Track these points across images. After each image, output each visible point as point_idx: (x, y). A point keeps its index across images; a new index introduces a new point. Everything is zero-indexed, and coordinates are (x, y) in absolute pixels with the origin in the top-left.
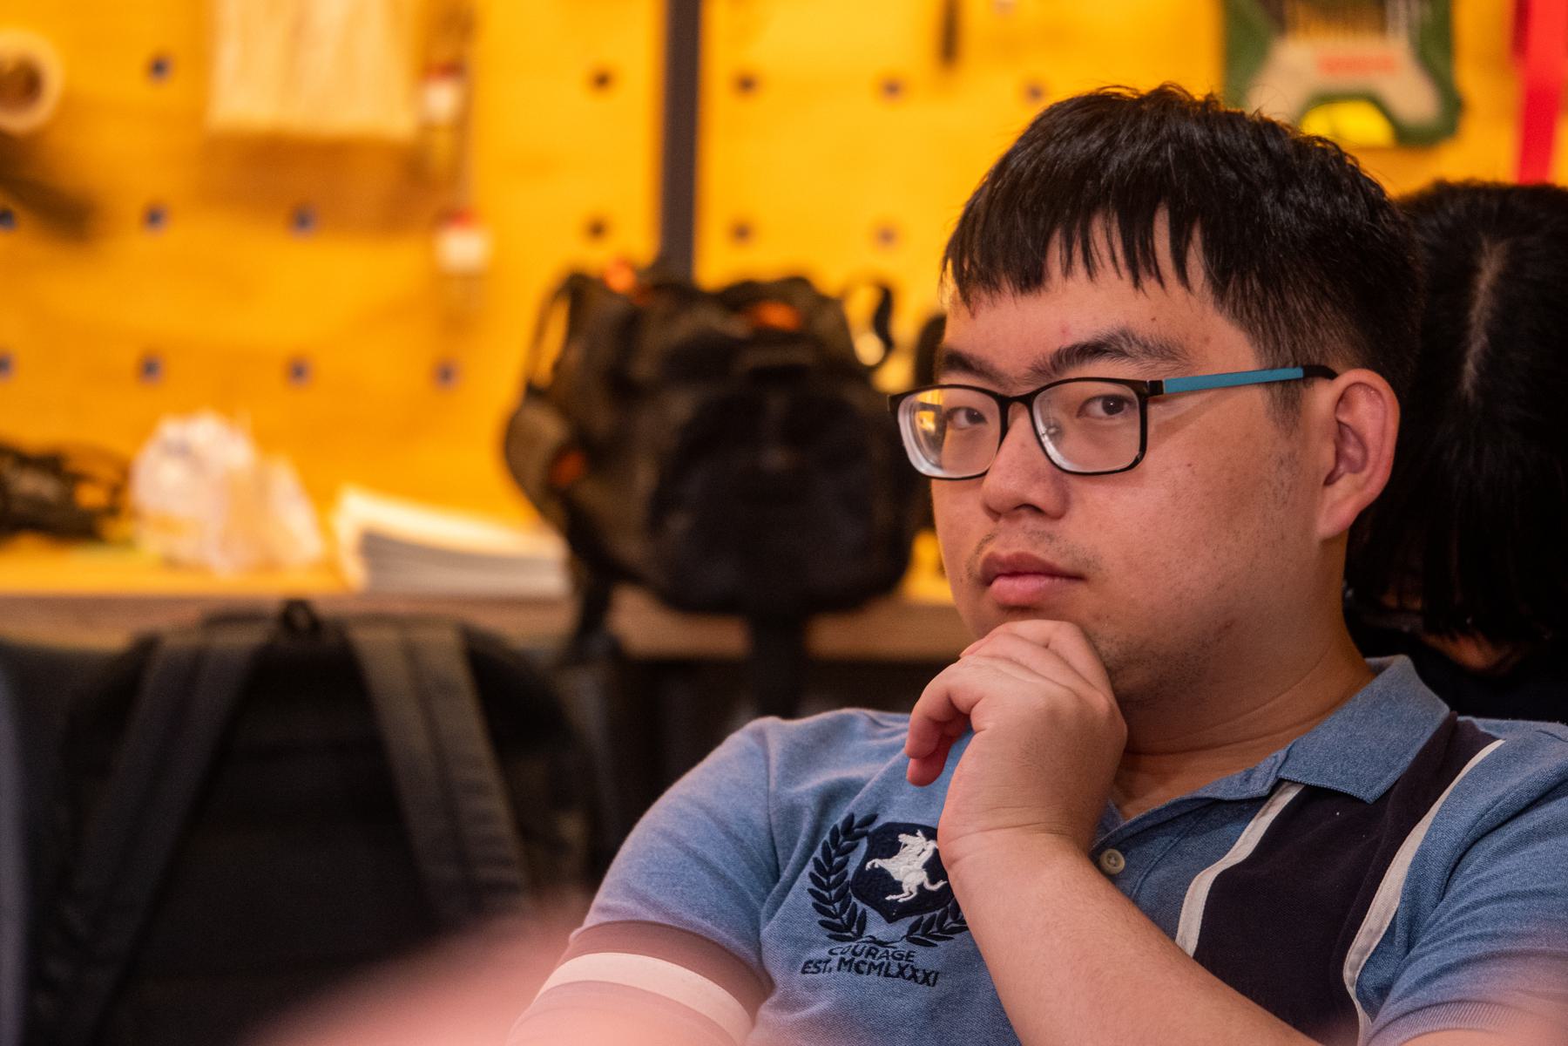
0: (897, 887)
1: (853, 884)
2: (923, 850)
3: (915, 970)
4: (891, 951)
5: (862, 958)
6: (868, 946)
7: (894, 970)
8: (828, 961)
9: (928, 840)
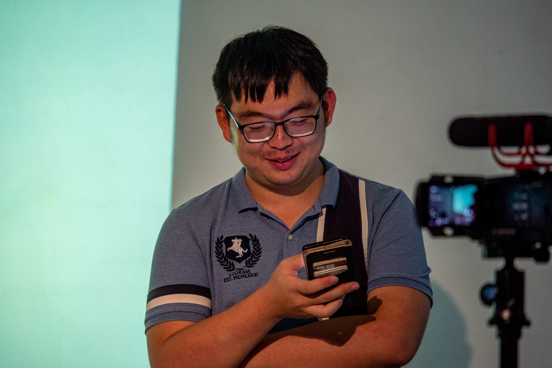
0: (238, 254)
1: (227, 255)
2: (238, 242)
3: (252, 274)
4: (244, 270)
5: (238, 275)
6: (238, 271)
7: (247, 276)
8: (230, 278)
9: (238, 239)
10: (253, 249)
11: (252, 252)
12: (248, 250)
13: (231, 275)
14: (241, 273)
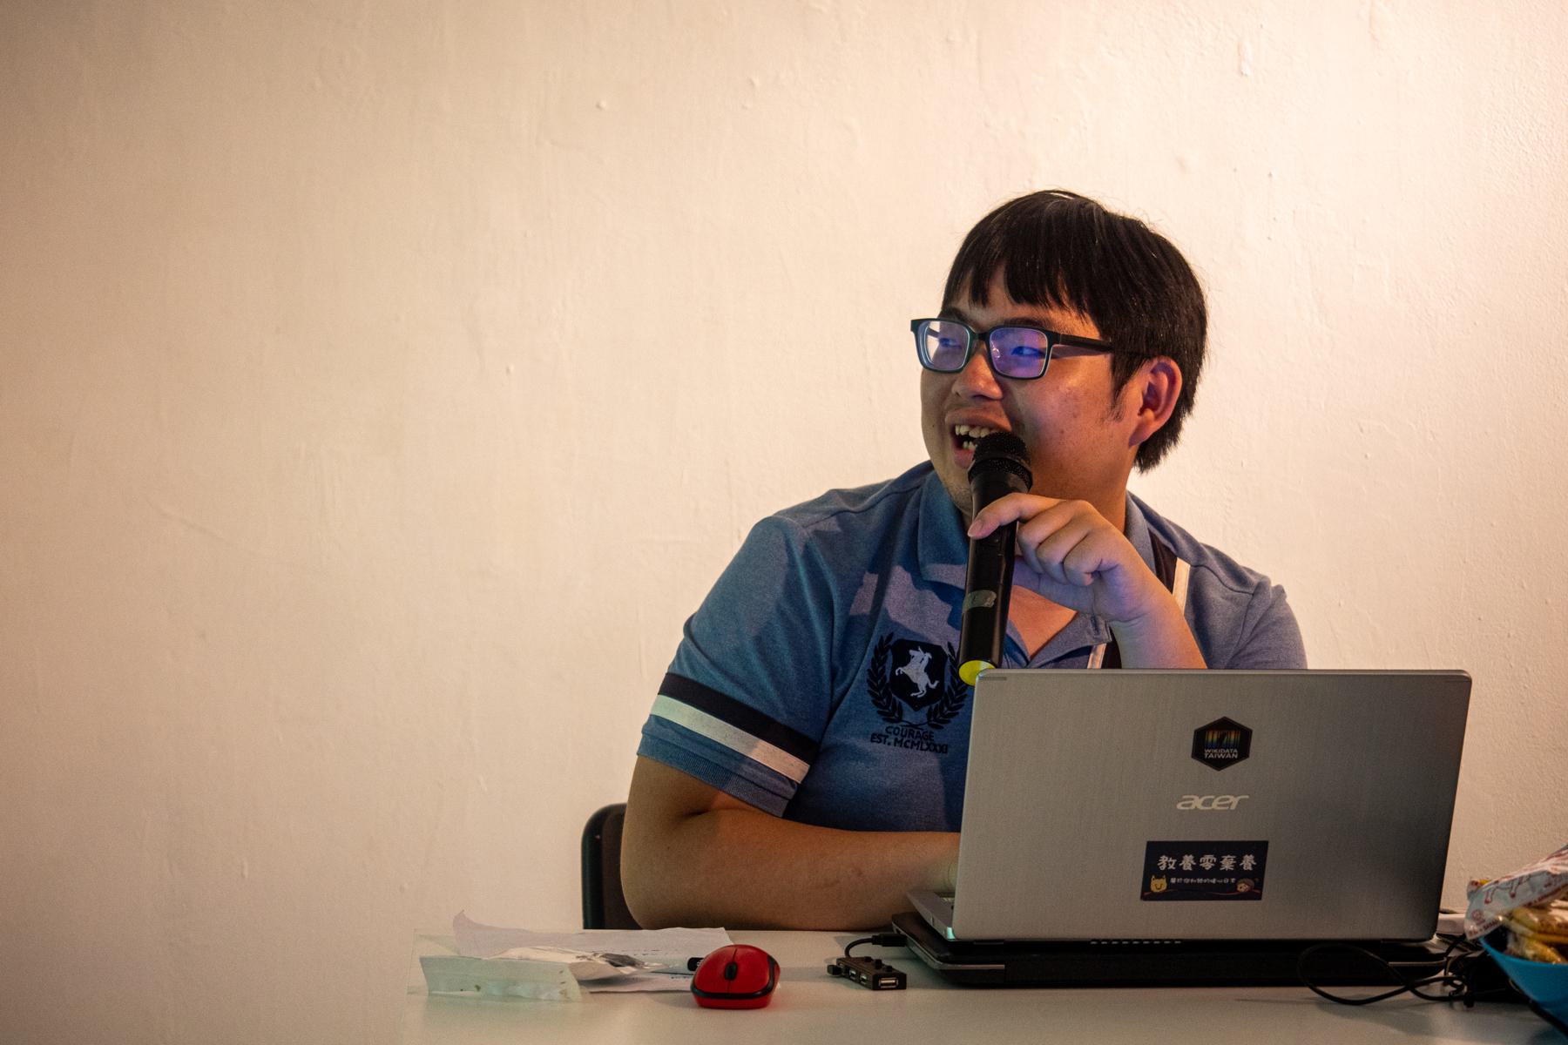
0: (915, 687)
3: (935, 745)
4: (921, 732)
6: (908, 728)
8: (887, 737)
10: (949, 684)
11: (946, 689)
12: (938, 685)
13: (890, 733)
14: (915, 735)
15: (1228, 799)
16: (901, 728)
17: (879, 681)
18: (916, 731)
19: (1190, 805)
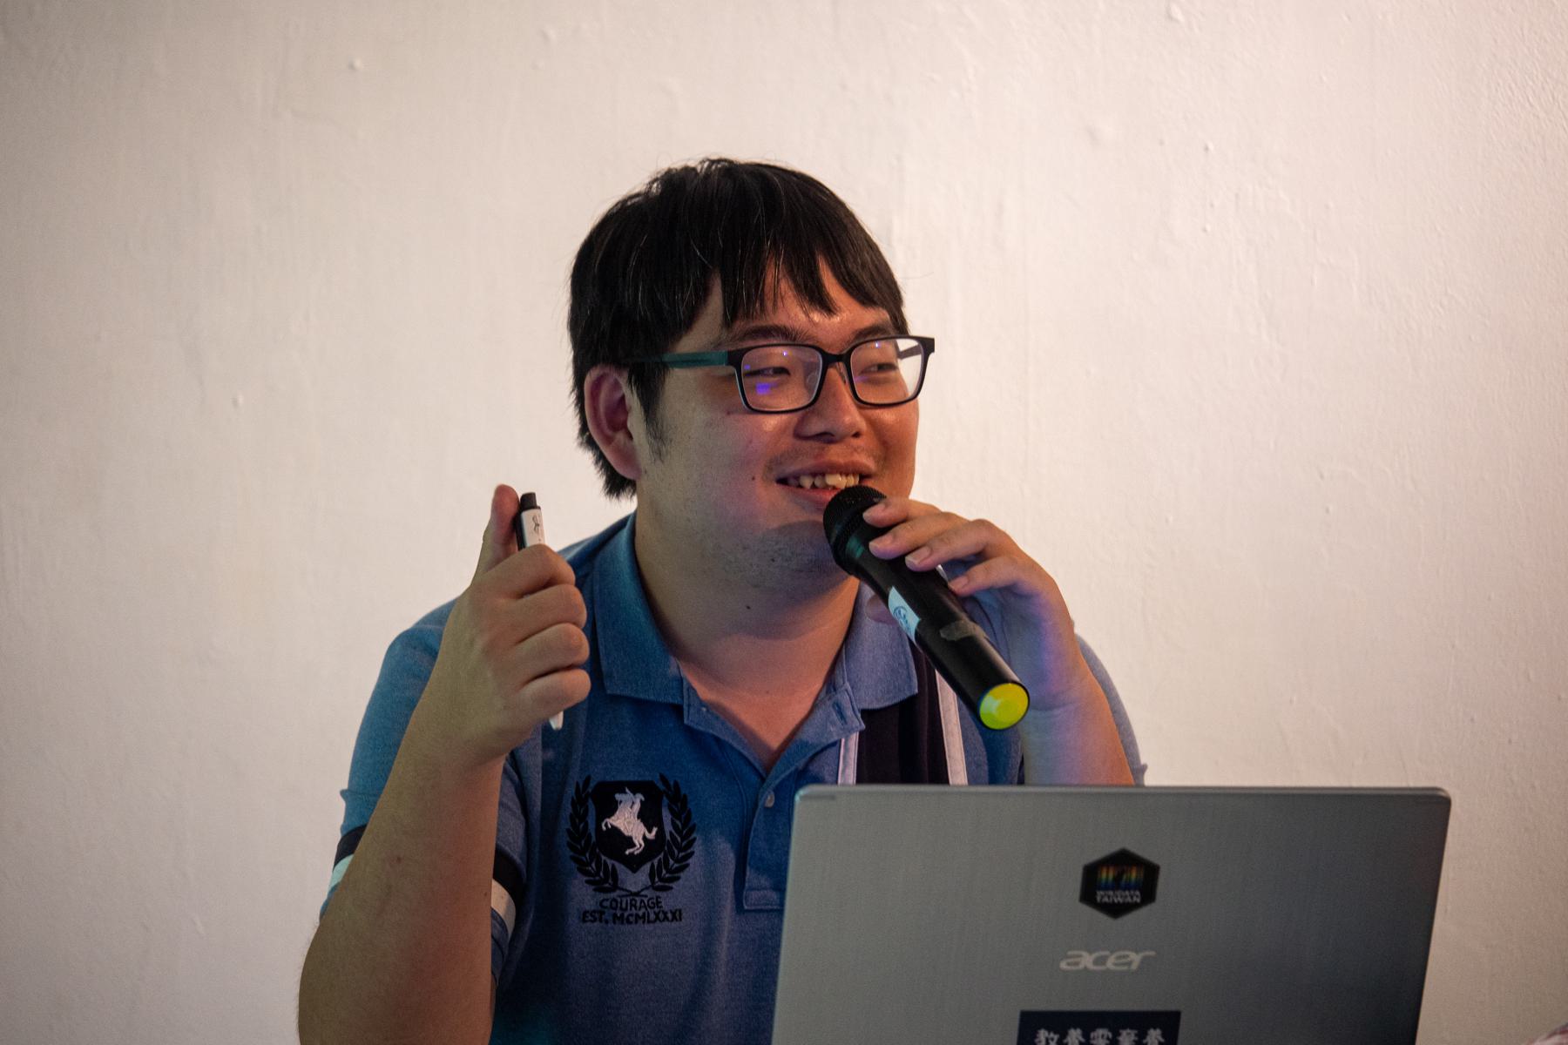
8: (602, 913)
15: (1128, 956)
16: (619, 900)
17: (583, 842)
18: (637, 899)
19: (1077, 964)
